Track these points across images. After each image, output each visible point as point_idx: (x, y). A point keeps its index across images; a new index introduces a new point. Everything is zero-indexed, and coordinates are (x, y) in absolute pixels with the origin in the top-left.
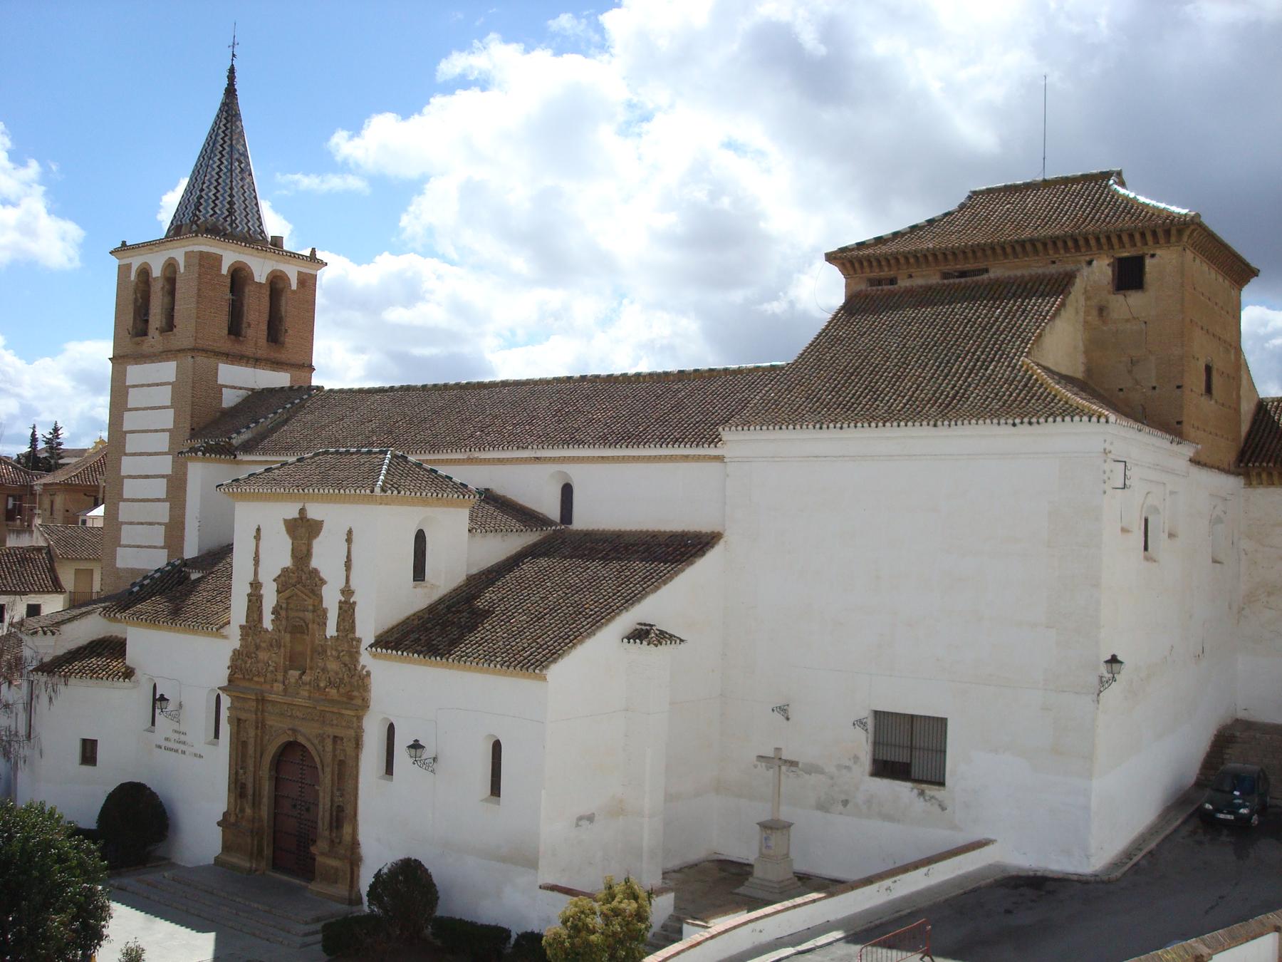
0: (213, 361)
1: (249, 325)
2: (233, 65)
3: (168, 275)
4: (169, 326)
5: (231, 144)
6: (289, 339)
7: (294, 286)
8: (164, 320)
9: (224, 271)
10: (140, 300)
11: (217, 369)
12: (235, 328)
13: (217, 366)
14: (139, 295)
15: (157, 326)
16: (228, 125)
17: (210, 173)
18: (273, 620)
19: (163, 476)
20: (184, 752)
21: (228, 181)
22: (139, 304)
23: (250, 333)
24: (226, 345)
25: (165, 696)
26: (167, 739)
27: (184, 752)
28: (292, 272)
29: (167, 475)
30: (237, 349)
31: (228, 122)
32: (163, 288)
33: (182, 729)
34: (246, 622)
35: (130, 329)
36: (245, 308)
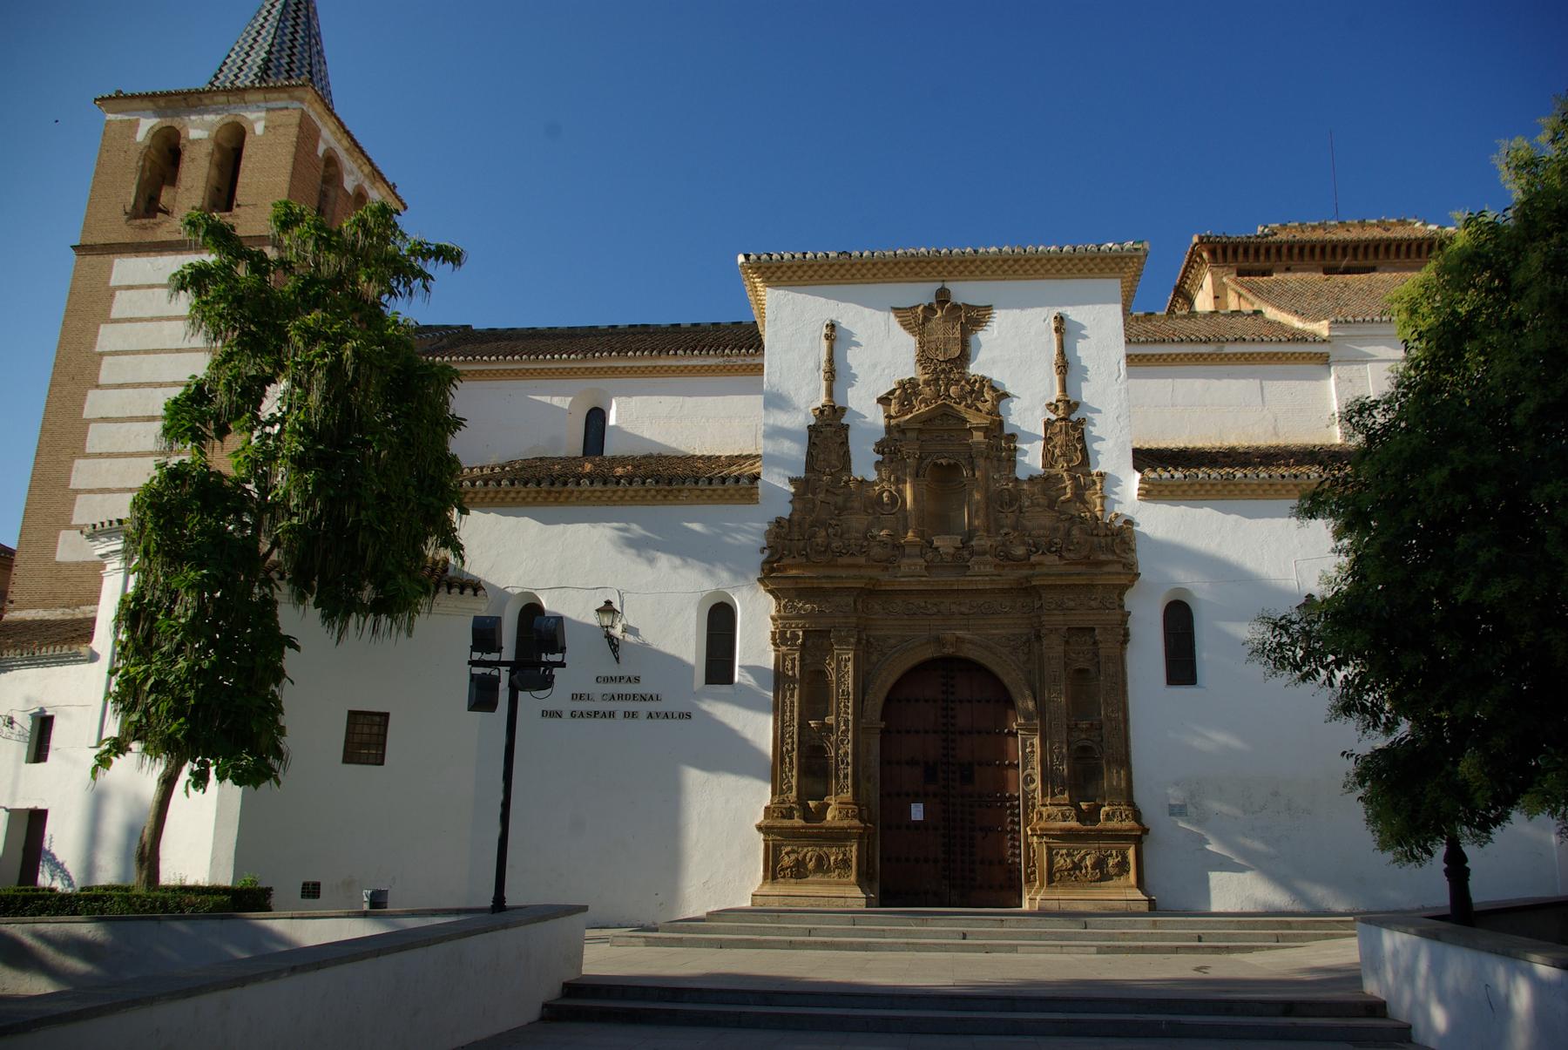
3: (220, 141)
8: (207, 200)
9: (320, 152)
10: (148, 173)
14: (147, 164)
15: (194, 204)
17: (280, 37)
18: (877, 462)
20: (633, 715)
21: (306, 55)
22: (145, 178)
26: (575, 697)
27: (633, 715)
32: (212, 154)
33: (624, 670)
35: (129, 209)
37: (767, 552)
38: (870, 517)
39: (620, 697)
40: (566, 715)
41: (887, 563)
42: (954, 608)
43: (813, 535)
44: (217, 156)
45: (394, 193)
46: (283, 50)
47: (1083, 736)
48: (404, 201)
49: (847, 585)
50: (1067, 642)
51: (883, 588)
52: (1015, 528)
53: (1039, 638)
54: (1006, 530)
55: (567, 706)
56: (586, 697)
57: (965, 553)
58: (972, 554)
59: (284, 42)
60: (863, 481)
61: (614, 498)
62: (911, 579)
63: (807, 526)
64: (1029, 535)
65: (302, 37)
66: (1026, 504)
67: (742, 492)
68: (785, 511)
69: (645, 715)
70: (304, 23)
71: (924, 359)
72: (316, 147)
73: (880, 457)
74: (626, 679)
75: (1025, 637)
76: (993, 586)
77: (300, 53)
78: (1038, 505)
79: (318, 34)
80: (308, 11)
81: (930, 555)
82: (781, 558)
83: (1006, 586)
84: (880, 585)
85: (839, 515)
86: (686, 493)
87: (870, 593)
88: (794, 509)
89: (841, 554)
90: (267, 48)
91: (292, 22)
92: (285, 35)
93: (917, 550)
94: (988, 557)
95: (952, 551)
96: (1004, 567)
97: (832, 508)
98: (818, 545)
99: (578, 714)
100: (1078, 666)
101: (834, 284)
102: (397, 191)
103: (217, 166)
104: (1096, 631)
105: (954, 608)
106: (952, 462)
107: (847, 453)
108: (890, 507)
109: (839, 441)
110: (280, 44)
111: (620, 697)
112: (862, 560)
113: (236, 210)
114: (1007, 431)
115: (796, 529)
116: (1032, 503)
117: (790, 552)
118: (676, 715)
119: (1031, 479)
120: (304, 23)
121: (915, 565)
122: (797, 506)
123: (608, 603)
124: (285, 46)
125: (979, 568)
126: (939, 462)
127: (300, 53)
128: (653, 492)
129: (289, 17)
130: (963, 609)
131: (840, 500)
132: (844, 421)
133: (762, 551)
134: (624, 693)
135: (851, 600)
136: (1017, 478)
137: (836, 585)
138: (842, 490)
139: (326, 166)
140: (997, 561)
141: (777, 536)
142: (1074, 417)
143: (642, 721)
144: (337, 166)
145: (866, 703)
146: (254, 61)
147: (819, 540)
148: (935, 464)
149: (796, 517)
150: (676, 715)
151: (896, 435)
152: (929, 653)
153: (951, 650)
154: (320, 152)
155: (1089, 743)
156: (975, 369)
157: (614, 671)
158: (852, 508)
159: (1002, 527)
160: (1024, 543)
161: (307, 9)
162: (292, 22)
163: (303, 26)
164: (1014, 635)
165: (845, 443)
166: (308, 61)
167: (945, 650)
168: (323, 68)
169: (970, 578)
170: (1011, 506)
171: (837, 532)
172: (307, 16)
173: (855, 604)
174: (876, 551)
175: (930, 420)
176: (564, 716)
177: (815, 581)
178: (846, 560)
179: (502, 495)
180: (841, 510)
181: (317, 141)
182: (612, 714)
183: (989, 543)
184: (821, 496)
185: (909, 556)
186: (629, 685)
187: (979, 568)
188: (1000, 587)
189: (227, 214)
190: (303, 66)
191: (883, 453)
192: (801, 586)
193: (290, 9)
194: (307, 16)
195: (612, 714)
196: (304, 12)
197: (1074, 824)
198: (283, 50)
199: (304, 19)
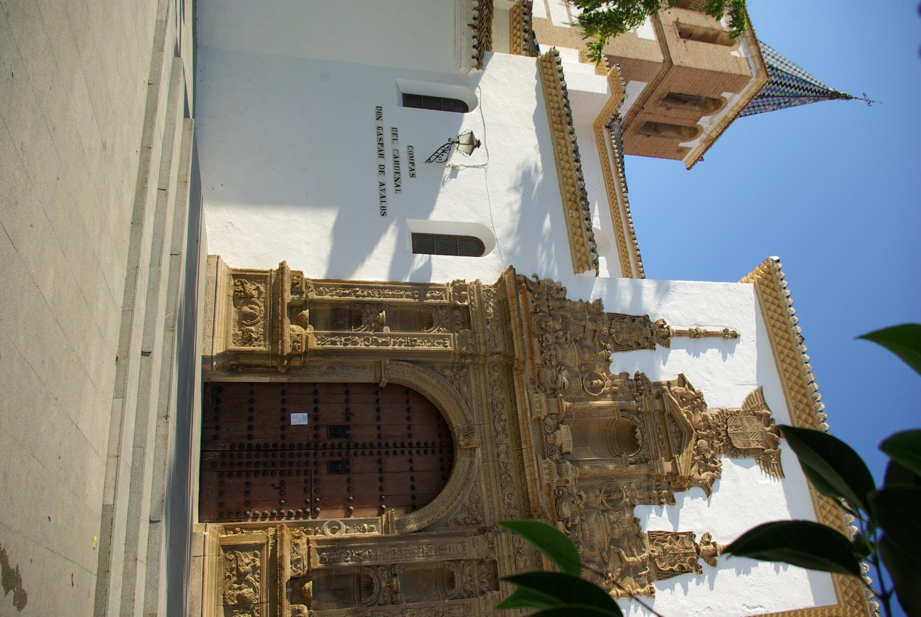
0: (653, 77)
1: (668, 109)
2: (852, 98)
3: (721, 35)
4: (686, 34)
5: (802, 96)
6: (641, 139)
7: (682, 145)
8: (684, 27)
9: (726, 95)
11: (643, 81)
12: (674, 98)
13: (646, 81)
16: (814, 94)
17: (787, 77)
18: (628, 375)
19: (548, 14)
20: (382, 171)
21: (778, 93)
23: (662, 110)
24: (661, 91)
25: (476, 149)
26: (395, 132)
27: (382, 171)
28: (694, 145)
29: (550, 19)
30: (654, 98)
31: (816, 93)
32: (713, 29)
34: (610, 314)
36: (682, 106)
37: (534, 280)
38: (577, 369)
39: (397, 163)
40: (379, 123)
41: (538, 383)
42: (503, 448)
43: (554, 318)
44: (711, 33)
45: (696, 161)
46: (780, 78)
47: (384, 584)
48: (693, 167)
49: (515, 342)
50: (481, 562)
51: (515, 378)
52: (586, 505)
53: (483, 531)
54: (584, 496)
55: (387, 124)
56: (395, 137)
57: (557, 456)
58: (557, 462)
59: (784, 79)
60: (608, 362)
61: (562, 163)
62: (527, 403)
63: (562, 313)
64: (582, 520)
65: (788, 91)
66: (612, 517)
67: (584, 258)
68: (573, 295)
69: (383, 180)
70: (797, 93)
71: (725, 416)
72: (728, 90)
73: (632, 377)
74: (413, 168)
75: (481, 519)
76: (529, 484)
77: (779, 90)
78: (613, 528)
79: (790, 106)
80: (803, 96)
81: (550, 422)
82: (530, 291)
83: (531, 497)
84: (518, 375)
85: (576, 341)
86: (575, 214)
87: (509, 367)
88: (575, 303)
89: (541, 342)
90: (780, 68)
91: (796, 86)
92: (789, 80)
93: (554, 410)
94: (556, 478)
95: (558, 442)
96: (549, 495)
97: (581, 335)
98: (546, 322)
99: (381, 132)
100: (457, 576)
101: (769, 337)
102: (699, 163)
103: (705, 34)
104: (495, 592)
105: (503, 448)
106: (640, 442)
107: (629, 348)
108: (589, 386)
109: (640, 341)
110: (783, 76)
111: (397, 163)
112: (538, 360)
113: (682, 41)
114: (677, 495)
115: (558, 304)
116: (614, 522)
117: (537, 299)
118: (384, 204)
119: (636, 521)
120: (797, 93)
121: (541, 406)
122: (578, 305)
123: (478, 144)
124: (782, 79)
125: (545, 469)
126: (638, 430)
127: (779, 90)
128: (572, 189)
129: (799, 84)
130: (502, 456)
131: (588, 342)
132: (657, 346)
133: (535, 276)
134: (401, 166)
135: (500, 349)
136: (634, 506)
137: (514, 332)
138: (597, 343)
139: (714, 100)
140: (554, 487)
141: (550, 288)
142: (701, 562)
143: (376, 178)
144: (715, 110)
145: (405, 363)
146: (770, 60)
147: (551, 323)
148: (634, 427)
149: (568, 303)
150: (384, 204)
151: (654, 391)
152: (457, 423)
153: (462, 443)
154: (726, 95)
155: (376, 590)
156: (726, 463)
157: (419, 159)
158: (583, 352)
159: (586, 493)
160: (574, 515)
161: (805, 96)
162: (796, 86)
163: (795, 92)
164: (482, 508)
165: (639, 346)
166: (775, 95)
167: (461, 437)
168: (771, 108)
169: (535, 458)
170: (608, 501)
171: (561, 339)
172: (801, 96)
173: (498, 353)
174: (548, 374)
175: (674, 421)
176: (378, 121)
177: (516, 313)
178: (536, 346)
179: (552, 85)
180: (579, 342)
181: (732, 91)
182: (381, 156)
183: (570, 479)
184: (590, 326)
185: (548, 402)
186: (407, 170)
187: (545, 469)
188: (530, 490)
189: (678, 36)
190: (772, 91)
191: (636, 380)
192: (510, 302)
193: (803, 84)
194: (801, 96)
195: (381, 156)
196: (803, 94)
197: (288, 573)
198: (780, 78)
199: (799, 93)
